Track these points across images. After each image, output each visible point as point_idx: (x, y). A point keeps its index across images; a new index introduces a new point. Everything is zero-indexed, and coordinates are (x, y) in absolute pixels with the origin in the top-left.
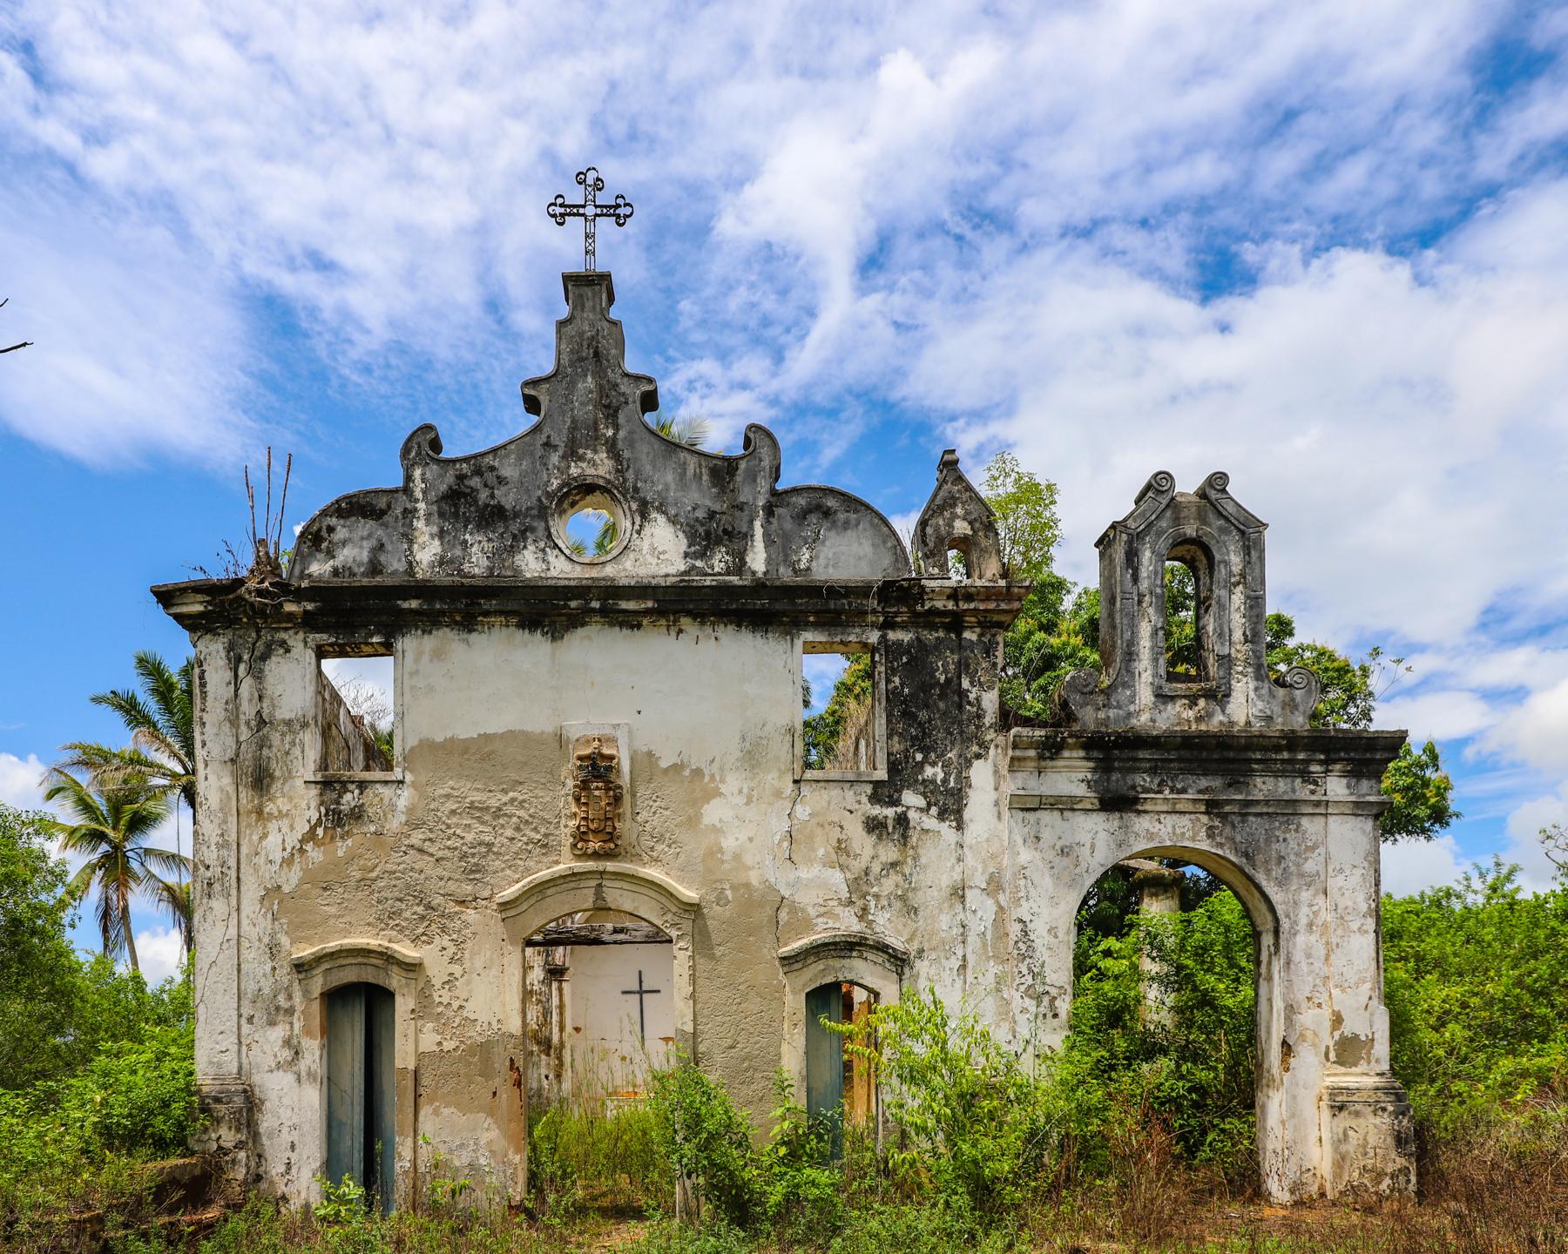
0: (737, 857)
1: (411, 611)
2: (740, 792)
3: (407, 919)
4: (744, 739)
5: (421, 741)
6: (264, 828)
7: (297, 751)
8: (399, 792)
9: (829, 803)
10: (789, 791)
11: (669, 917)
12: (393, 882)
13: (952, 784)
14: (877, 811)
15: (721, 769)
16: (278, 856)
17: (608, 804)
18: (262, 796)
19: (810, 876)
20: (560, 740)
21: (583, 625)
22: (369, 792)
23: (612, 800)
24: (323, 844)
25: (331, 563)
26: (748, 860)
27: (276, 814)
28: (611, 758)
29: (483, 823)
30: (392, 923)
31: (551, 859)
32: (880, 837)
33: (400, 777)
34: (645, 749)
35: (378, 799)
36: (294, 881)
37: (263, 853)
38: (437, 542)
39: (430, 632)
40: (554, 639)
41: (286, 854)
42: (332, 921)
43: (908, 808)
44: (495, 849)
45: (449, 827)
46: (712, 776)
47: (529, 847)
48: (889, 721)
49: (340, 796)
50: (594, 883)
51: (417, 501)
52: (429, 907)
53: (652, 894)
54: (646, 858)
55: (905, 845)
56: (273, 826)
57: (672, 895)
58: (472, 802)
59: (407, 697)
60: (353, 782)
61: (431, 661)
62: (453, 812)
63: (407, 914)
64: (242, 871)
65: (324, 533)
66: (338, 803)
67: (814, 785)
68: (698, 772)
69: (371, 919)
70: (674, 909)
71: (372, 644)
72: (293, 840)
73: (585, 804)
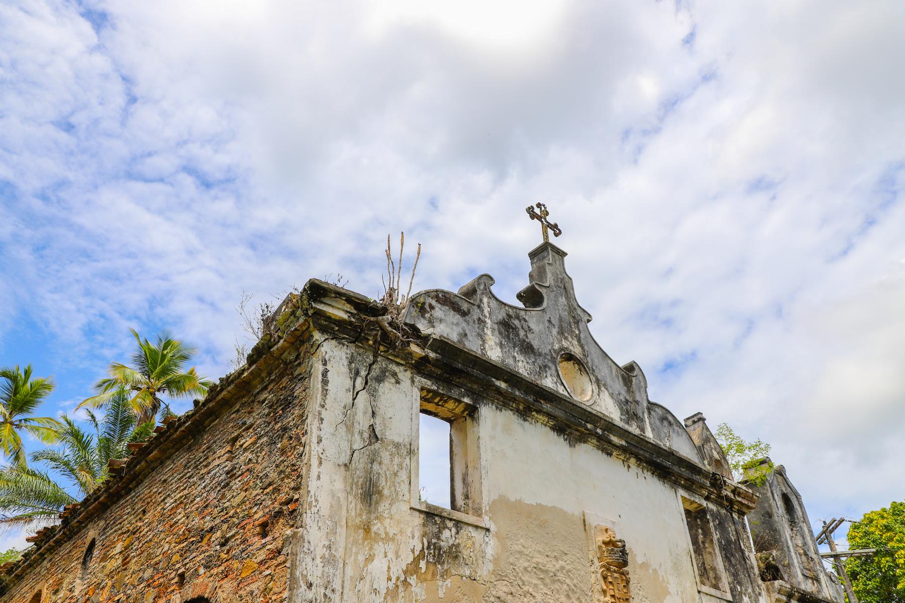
6: (371, 548)
8: (487, 539)
16: (382, 585)
18: (370, 512)
21: (585, 442)
24: (426, 580)
27: (383, 536)
35: (470, 542)
37: (368, 579)
38: (499, 349)
40: (570, 445)
41: (391, 585)
51: (485, 316)
56: (379, 548)
60: (451, 520)
64: (345, 597)
66: (439, 538)
72: (397, 570)
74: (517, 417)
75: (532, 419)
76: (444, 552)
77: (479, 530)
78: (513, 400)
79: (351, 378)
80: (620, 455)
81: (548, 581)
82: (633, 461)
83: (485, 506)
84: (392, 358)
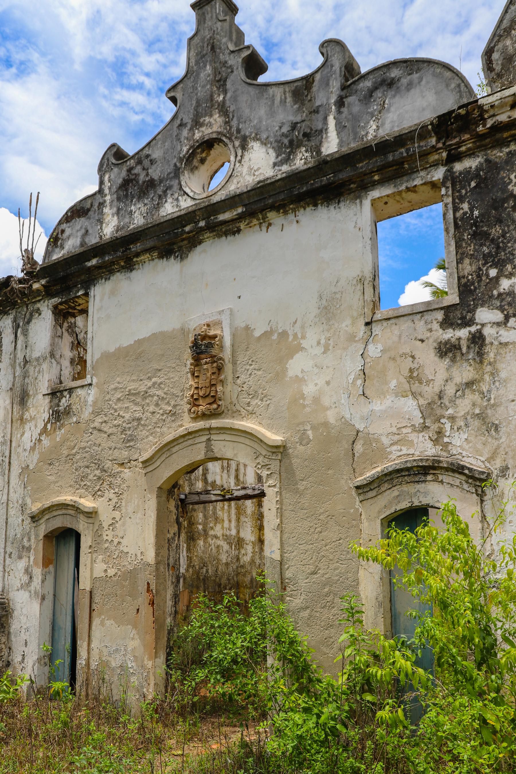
0: (316, 400)
2: (319, 343)
3: (90, 480)
4: (321, 298)
5: (102, 354)
7: (40, 377)
8: (89, 392)
9: (400, 337)
11: (260, 459)
12: (84, 455)
14: (449, 334)
15: (303, 327)
17: (213, 373)
19: (383, 407)
21: (200, 243)
23: (215, 370)
25: (62, 252)
26: (326, 401)
29: (136, 404)
30: (83, 483)
31: (177, 424)
32: (453, 360)
33: (89, 382)
34: (243, 325)
35: (78, 399)
36: (35, 461)
39: (109, 279)
42: (52, 486)
43: (483, 325)
44: (142, 422)
45: (116, 411)
46: (295, 335)
47: (164, 418)
49: (60, 401)
50: (204, 438)
52: (104, 470)
53: (248, 442)
54: (243, 412)
55: (481, 362)
57: (261, 441)
58: (130, 390)
60: (66, 390)
61: (109, 298)
62: (119, 400)
63: (91, 477)
65: (60, 236)
66: (58, 406)
67: (385, 323)
68: (284, 334)
69: (72, 483)
70: (264, 453)
73: (198, 377)
75: (139, 264)
76: (62, 413)
80: (251, 222)
81: (139, 400)
82: (271, 215)
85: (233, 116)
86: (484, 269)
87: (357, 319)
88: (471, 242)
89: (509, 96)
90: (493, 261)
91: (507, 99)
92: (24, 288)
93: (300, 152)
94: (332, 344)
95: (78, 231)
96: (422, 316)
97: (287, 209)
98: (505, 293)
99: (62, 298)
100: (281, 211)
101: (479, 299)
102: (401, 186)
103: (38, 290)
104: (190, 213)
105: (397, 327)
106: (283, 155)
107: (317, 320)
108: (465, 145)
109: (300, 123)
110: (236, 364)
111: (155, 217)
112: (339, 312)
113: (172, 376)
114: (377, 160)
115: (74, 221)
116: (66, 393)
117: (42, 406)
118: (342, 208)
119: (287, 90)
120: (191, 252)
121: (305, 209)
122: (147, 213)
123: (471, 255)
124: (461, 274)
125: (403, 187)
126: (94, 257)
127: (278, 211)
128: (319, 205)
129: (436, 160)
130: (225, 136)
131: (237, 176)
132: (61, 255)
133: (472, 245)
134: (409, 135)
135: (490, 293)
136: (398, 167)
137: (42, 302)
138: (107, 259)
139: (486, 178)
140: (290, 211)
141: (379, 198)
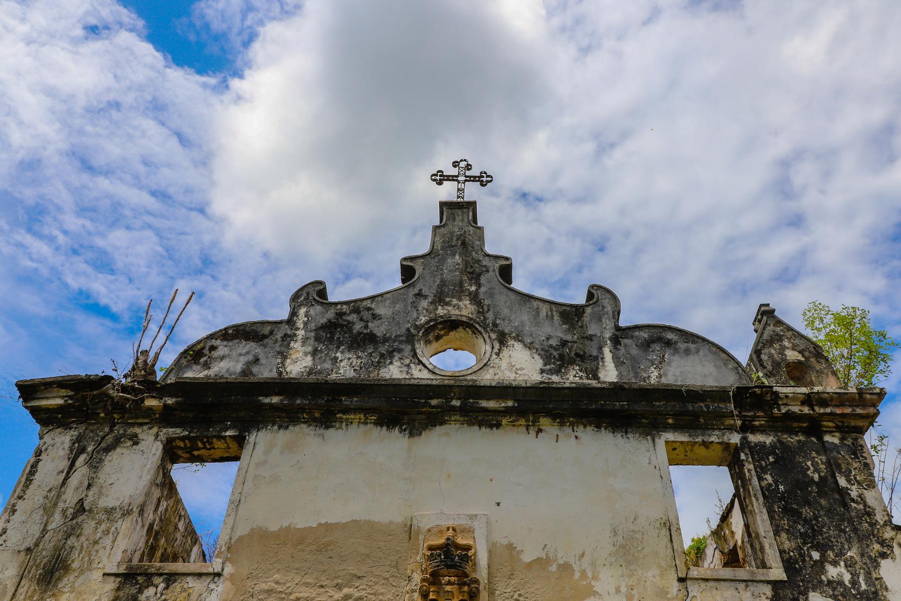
1: (271, 406)
2: (618, 591)
5: (252, 530)
7: (108, 541)
8: (212, 586)
10: (675, 591)
13: (864, 587)
15: (593, 564)
20: (410, 531)
21: (441, 424)
22: (177, 587)
25: (206, 372)
28: (468, 548)
33: (218, 569)
34: (505, 542)
35: (185, 594)
39: (287, 428)
46: (583, 573)
48: (771, 518)
51: (297, 329)
59: (249, 484)
61: (282, 452)
65: (206, 351)
67: (703, 584)
68: (566, 568)
71: (224, 438)
74: (314, 428)
75: (342, 422)
77: (204, 578)
78: (300, 411)
79: (69, 459)
83: (221, 547)
84: (133, 421)
85: (489, 310)
86: (805, 548)
87: (666, 570)
88: (784, 516)
89: (800, 393)
90: (812, 542)
91: (799, 395)
92: (127, 400)
93: (573, 369)
94: (636, 596)
95: (240, 355)
96: (747, 586)
97: (566, 420)
98: (835, 582)
99: (190, 432)
100: (558, 420)
101: (808, 582)
102: (697, 438)
103: (150, 409)
104: (444, 386)
105: (719, 592)
106: (552, 366)
107: (613, 559)
108: (758, 421)
109: (571, 342)
110: (493, 594)
111: (372, 375)
112: (642, 556)
113: (382, 591)
114: (675, 405)
115: (236, 341)
116: (157, 580)
117: (94, 594)
118: (632, 439)
119: (554, 309)
120: (427, 431)
121: (585, 427)
122: (361, 368)
123: (786, 529)
124: (781, 547)
125: (699, 439)
126: (277, 394)
127: (554, 419)
128: (602, 429)
129: (731, 425)
130: (477, 323)
131: (493, 367)
132: (201, 375)
133: (785, 519)
134: (711, 393)
135: (818, 577)
136: (693, 418)
137: (145, 428)
138: (299, 402)
139: (783, 457)
140: (568, 424)
141: (672, 442)
